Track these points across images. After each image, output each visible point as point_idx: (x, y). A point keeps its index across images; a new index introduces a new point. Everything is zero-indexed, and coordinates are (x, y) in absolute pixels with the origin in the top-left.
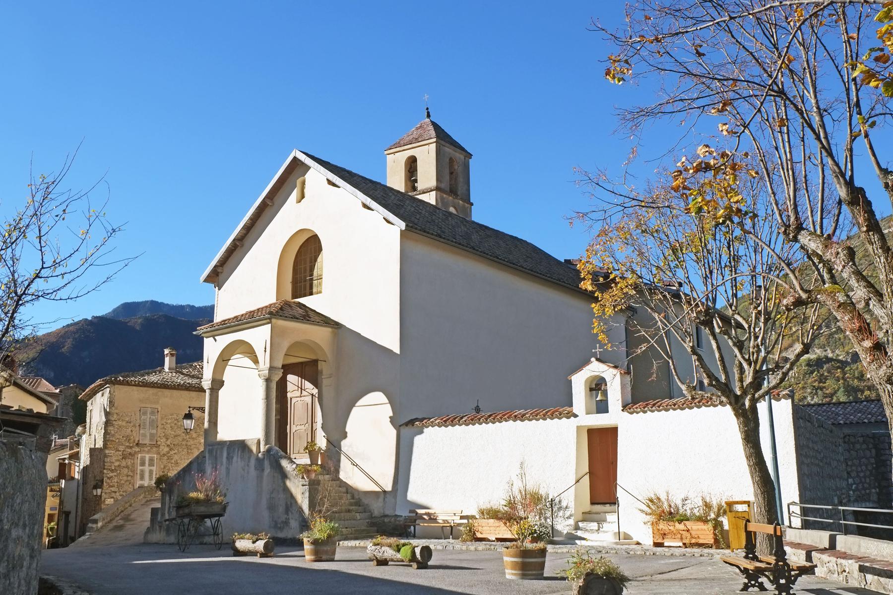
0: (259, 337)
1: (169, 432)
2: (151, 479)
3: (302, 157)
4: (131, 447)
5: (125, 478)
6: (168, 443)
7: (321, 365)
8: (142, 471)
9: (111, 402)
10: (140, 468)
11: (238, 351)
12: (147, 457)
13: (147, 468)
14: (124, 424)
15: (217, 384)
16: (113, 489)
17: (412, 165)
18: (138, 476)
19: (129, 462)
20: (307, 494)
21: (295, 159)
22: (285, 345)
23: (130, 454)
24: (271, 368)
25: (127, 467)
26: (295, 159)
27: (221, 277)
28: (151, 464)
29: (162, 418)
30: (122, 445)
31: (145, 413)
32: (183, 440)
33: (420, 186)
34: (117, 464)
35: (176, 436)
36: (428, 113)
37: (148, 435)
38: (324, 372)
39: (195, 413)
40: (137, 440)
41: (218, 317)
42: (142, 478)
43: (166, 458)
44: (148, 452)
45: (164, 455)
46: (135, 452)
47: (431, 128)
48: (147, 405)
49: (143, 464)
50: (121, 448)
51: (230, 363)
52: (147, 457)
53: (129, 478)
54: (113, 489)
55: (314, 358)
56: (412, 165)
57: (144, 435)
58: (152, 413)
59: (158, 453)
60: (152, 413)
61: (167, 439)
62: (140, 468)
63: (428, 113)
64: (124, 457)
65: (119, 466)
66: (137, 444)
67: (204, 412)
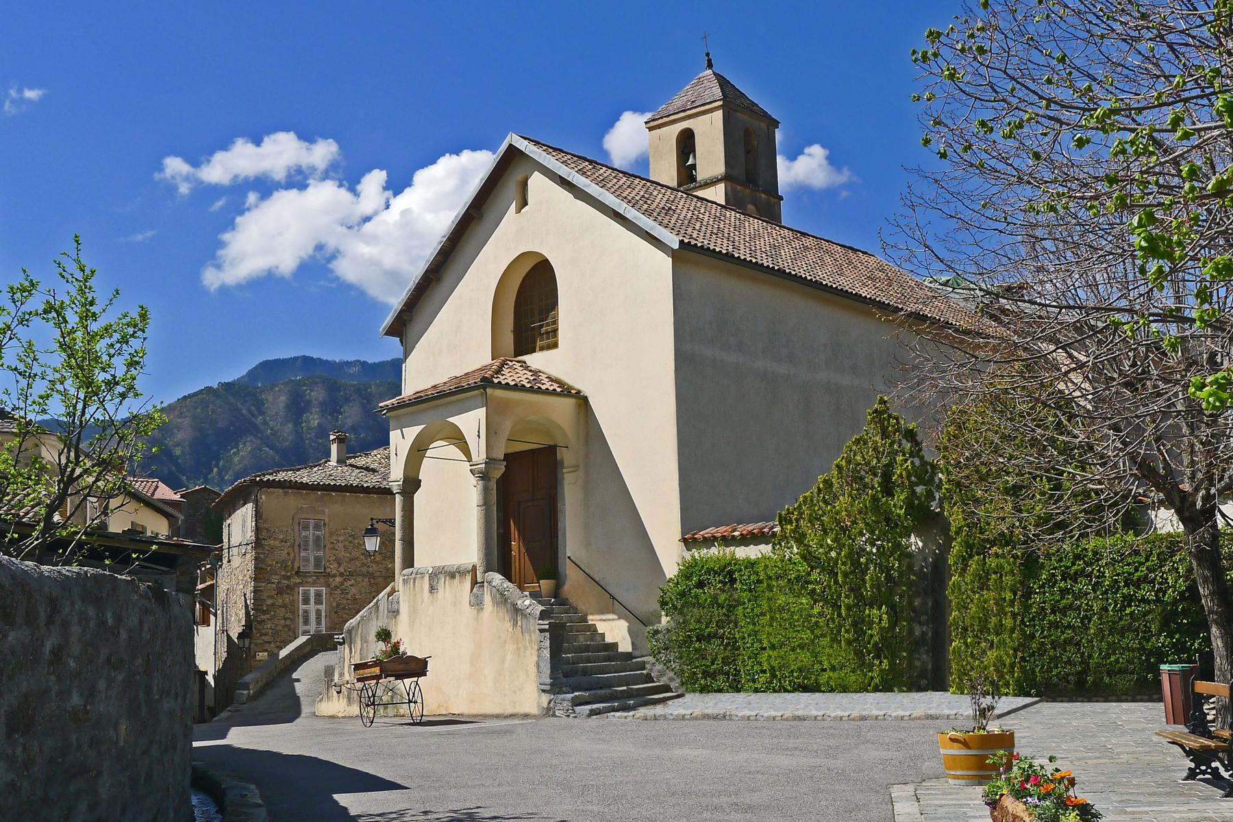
0: (471, 422)
1: (342, 554)
2: (319, 622)
3: (522, 145)
4: (288, 578)
5: (282, 622)
6: (342, 570)
7: (562, 454)
8: (306, 612)
9: (258, 515)
10: (302, 607)
11: (439, 436)
12: (312, 590)
13: (312, 607)
14: (277, 543)
15: (412, 484)
16: (266, 638)
17: (686, 143)
18: (301, 620)
19: (287, 599)
20: (547, 643)
21: (511, 147)
22: (507, 426)
23: (288, 586)
24: (490, 461)
25: (284, 606)
26: (511, 147)
27: (412, 331)
28: (318, 600)
29: (331, 534)
30: (276, 574)
31: (306, 528)
32: (363, 565)
33: (702, 174)
34: (270, 602)
35: (351, 560)
36: (709, 61)
37: (312, 559)
38: (566, 464)
39: (380, 527)
40: (296, 565)
41: (409, 389)
42: (306, 622)
43: (338, 591)
44: (314, 584)
45: (336, 587)
46: (295, 584)
47: (715, 84)
48: (308, 516)
49: (306, 601)
50: (275, 579)
51: (429, 453)
52: (312, 590)
53: (288, 622)
54: (266, 638)
55: (548, 442)
56: (686, 143)
57: (307, 560)
58: (317, 527)
59: (328, 585)
60: (317, 527)
61: (340, 564)
62: (302, 607)
63: (709, 61)
64: (280, 592)
65: (273, 605)
66: (297, 573)
67: (393, 524)
